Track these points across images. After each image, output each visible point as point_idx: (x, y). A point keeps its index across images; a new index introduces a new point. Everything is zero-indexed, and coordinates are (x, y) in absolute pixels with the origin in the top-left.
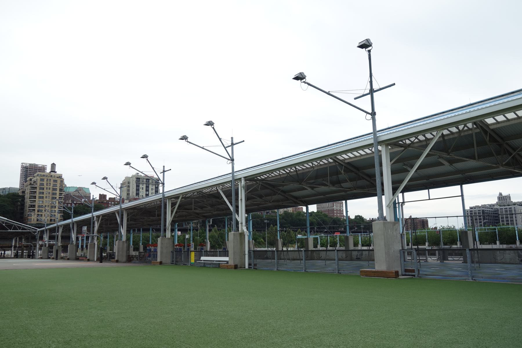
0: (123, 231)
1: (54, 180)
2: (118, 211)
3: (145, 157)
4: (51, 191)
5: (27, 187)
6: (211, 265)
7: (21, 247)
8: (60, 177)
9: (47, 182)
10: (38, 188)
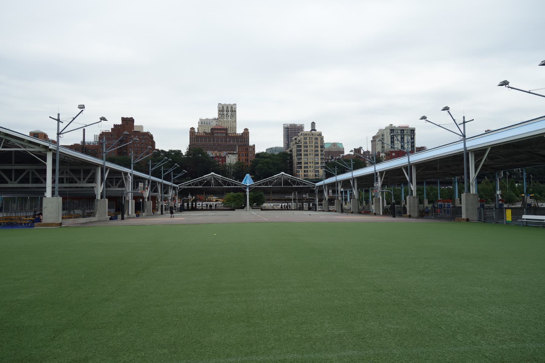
0: (413, 187)
1: (315, 138)
2: (406, 167)
3: (446, 109)
4: (313, 148)
5: (294, 146)
6: (540, 225)
7: (300, 200)
8: (320, 134)
9: (310, 140)
10: (303, 147)
